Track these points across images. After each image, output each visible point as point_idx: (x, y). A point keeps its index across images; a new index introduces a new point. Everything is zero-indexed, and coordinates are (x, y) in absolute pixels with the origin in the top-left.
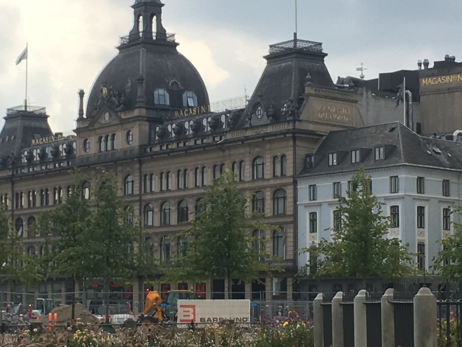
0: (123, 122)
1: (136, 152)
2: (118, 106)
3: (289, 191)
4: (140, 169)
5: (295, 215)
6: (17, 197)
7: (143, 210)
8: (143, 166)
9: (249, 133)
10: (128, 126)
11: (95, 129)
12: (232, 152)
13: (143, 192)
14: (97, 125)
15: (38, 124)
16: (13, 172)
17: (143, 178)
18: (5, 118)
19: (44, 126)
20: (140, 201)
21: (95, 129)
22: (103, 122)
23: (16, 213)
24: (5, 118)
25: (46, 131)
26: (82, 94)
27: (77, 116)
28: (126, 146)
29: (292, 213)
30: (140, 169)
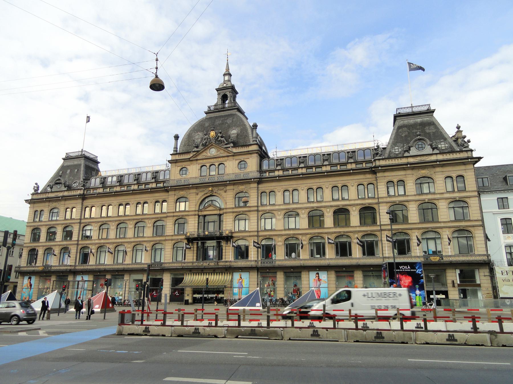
0: (235, 155)
1: (257, 175)
2: (226, 144)
3: (473, 202)
4: (258, 188)
5: (482, 220)
6: (83, 209)
7: (260, 218)
8: (260, 186)
9: (411, 160)
10: (242, 157)
11: (197, 160)
12: (386, 174)
13: (260, 204)
14: (199, 158)
15: (93, 166)
16: (84, 191)
17: (260, 195)
18: (64, 159)
19: (96, 167)
20: (258, 211)
21: (197, 160)
22: (209, 155)
23: (82, 221)
24: (64, 159)
25: (98, 171)
26: (177, 137)
27: (172, 152)
28: (237, 171)
29: (480, 218)
30: (258, 188)
